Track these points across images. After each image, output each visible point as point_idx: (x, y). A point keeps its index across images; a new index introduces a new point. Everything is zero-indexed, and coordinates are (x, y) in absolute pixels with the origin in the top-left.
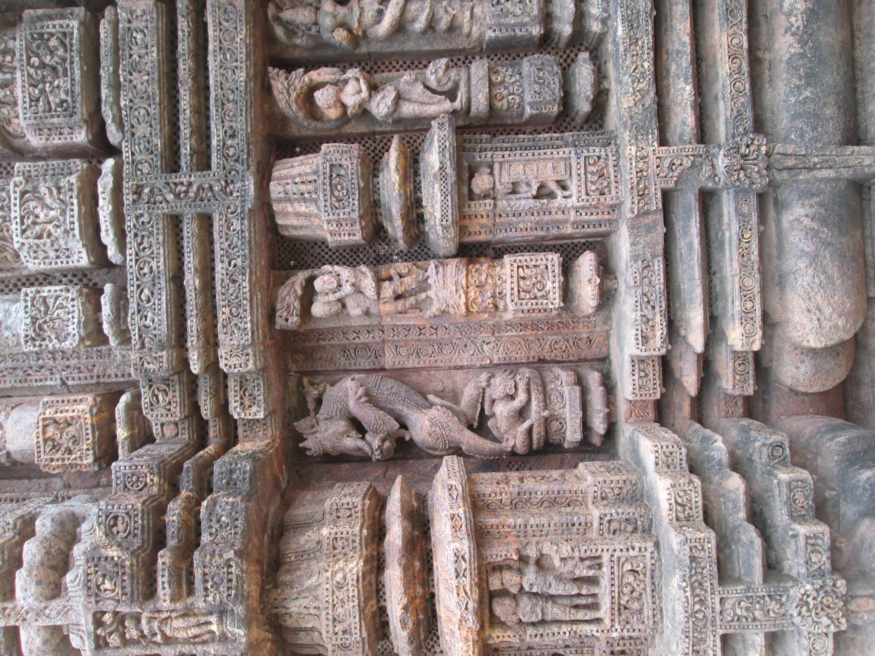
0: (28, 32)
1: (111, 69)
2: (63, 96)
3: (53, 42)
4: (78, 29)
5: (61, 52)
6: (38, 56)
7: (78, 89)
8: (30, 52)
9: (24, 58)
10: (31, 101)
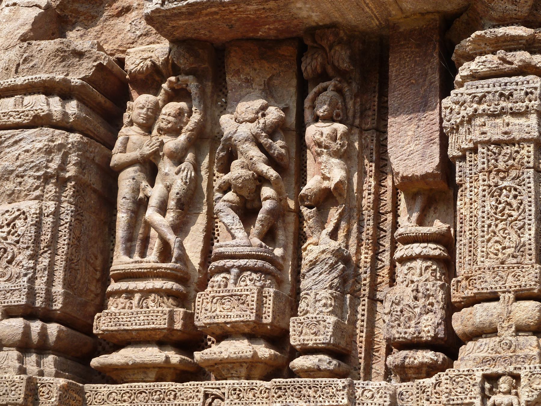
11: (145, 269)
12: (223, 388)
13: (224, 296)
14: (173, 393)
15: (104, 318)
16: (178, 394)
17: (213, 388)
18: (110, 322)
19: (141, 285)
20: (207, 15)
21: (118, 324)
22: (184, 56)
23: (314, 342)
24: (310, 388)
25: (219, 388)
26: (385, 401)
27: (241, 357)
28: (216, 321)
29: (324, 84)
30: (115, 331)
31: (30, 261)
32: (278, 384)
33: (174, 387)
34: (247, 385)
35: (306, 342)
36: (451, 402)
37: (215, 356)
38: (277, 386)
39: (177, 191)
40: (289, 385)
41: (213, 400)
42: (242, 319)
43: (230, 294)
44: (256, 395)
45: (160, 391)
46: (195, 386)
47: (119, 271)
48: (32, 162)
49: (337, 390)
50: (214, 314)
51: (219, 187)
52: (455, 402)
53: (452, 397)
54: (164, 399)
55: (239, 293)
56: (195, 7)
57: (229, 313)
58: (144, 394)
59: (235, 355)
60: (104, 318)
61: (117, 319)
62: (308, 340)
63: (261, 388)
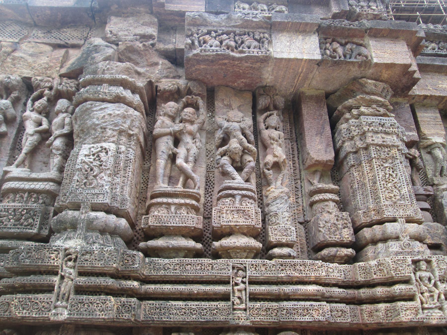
0: (38, 210)
1: (10, 246)
2: (5, 223)
3: (31, 221)
4: (32, 232)
5: (26, 223)
6: (27, 213)
7: (5, 230)
8: (28, 211)
9: (27, 207)
10: (8, 209)
11: (178, 191)
12: (245, 263)
13: (233, 211)
14: (211, 266)
16: (215, 266)
17: (238, 264)
19: (176, 201)
20: (220, 64)
22: (197, 86)
24: (301, 265)
25: (242, 264)
26: (341, 275)
27: (248, 245)
28: (230, 224)
29: (271, 112)
30: (159, 226)
31: (110, 178)
33: (211, 262)
34: (260, 262)
35: (280, 240)
36: (397, 275)
37: (231, 245)
39: (194, 152)
41: (238, 270)
42: (247, 224)
43: (237, 209)
44: (268, 269)
45: (201, 264)
46: (226, 262)
48: (113, 121)
49: (318, 267)
50: (228, 220)
51: (220, 153)
52: (400, 275)
53: (398, 272)
54: (204, 269)
55: (243, 209)
56: (218, 57)
57: (238, 220)
58: (189, 266)
59: (244, 245)
61: (160, 219)
62: (281, 239)
63: (270, 265)
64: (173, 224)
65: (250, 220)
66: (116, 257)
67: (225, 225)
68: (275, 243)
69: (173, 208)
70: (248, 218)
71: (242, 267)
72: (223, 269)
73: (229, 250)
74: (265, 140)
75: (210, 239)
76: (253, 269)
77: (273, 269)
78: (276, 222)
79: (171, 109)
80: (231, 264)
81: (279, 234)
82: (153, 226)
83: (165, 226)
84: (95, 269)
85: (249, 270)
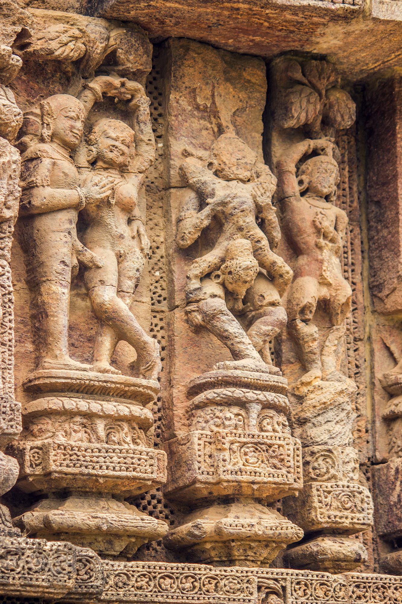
11: (113, 382)
12: (283, 579)
13: (245, 443)
15: (54, 453)
16: (222, 583)
17: (268, 579)
18: (64, 460)
21: (78, 465)
22: (136, 50)
23: (349, 520)
24: (396, 589)
25: (276, 580)
28: (239, 478)
32: (357, 580)
33: (213, 572)
35: (338, 519)
37: (243, 530)
38: (354, 582)
39: (136, 266)
40: (369, 583)
42: (277, 480)
43: (255, 440)
44: (330, 594)
45: (193, 577)
47: (69, 381)
50: (236, 468)
54: (200, 589)
55: (269, 442)
60: (54, 453)
62: (341, 518)
63: (334, 585)
64: (106, 472)
65: (284, 471)
66: (70, 566)
67: (228, 481)
68: (325, 525)
69: (101, 427)
70: (279, 465)
71: (278, 587)
72: (239, 590)
73: (233, 541)
74: (300, 231)
75: (159, 502)
76: (301, 593)
77: (341, 594)
78: (328, 472)
79: (71, 122)
80: (257, 580)
81: (335, 504)
82: (60, 472)
83: (89, 474)
84: (37, 589)
85: (292, 595)
